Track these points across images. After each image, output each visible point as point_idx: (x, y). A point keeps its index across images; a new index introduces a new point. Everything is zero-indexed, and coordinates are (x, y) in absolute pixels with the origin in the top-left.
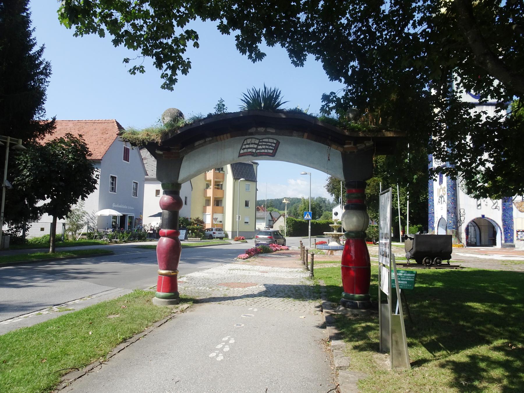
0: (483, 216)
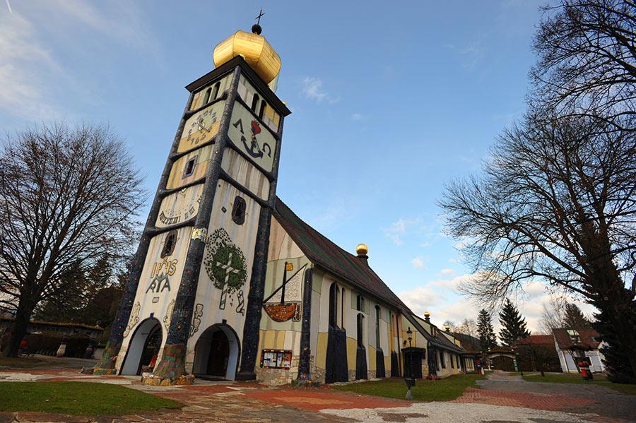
0: (224, 321)
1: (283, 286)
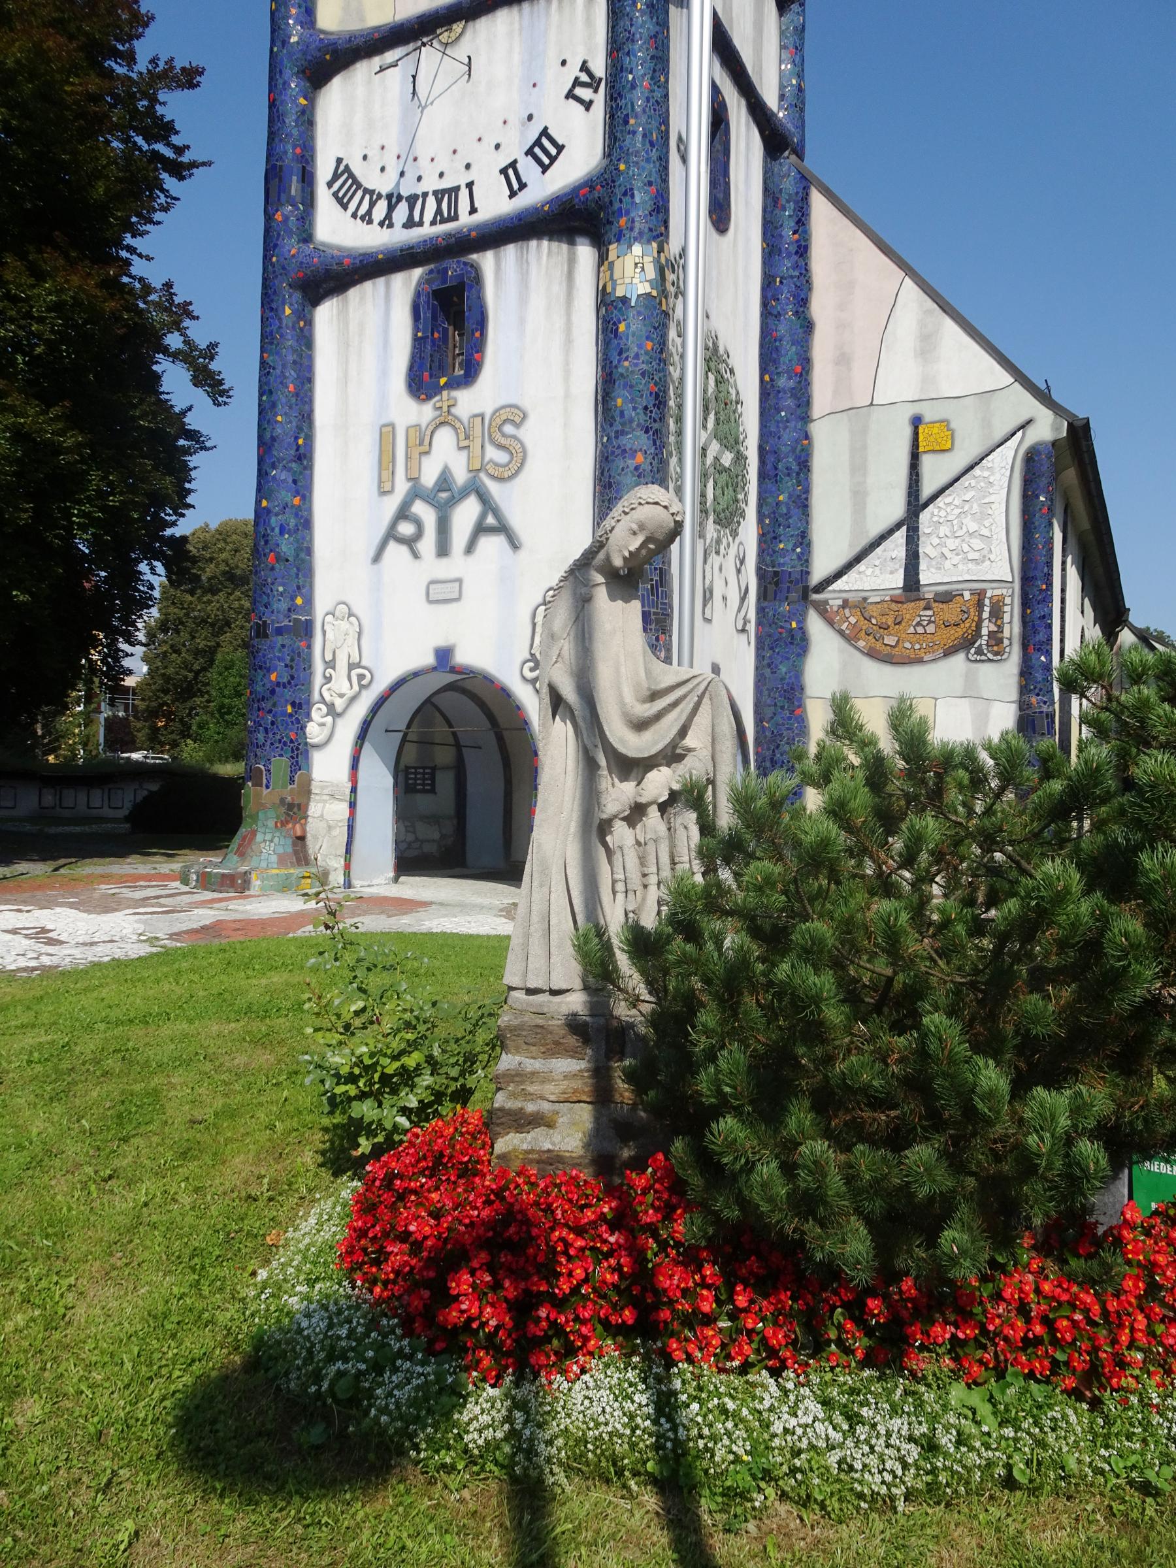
1: (910, 522)
